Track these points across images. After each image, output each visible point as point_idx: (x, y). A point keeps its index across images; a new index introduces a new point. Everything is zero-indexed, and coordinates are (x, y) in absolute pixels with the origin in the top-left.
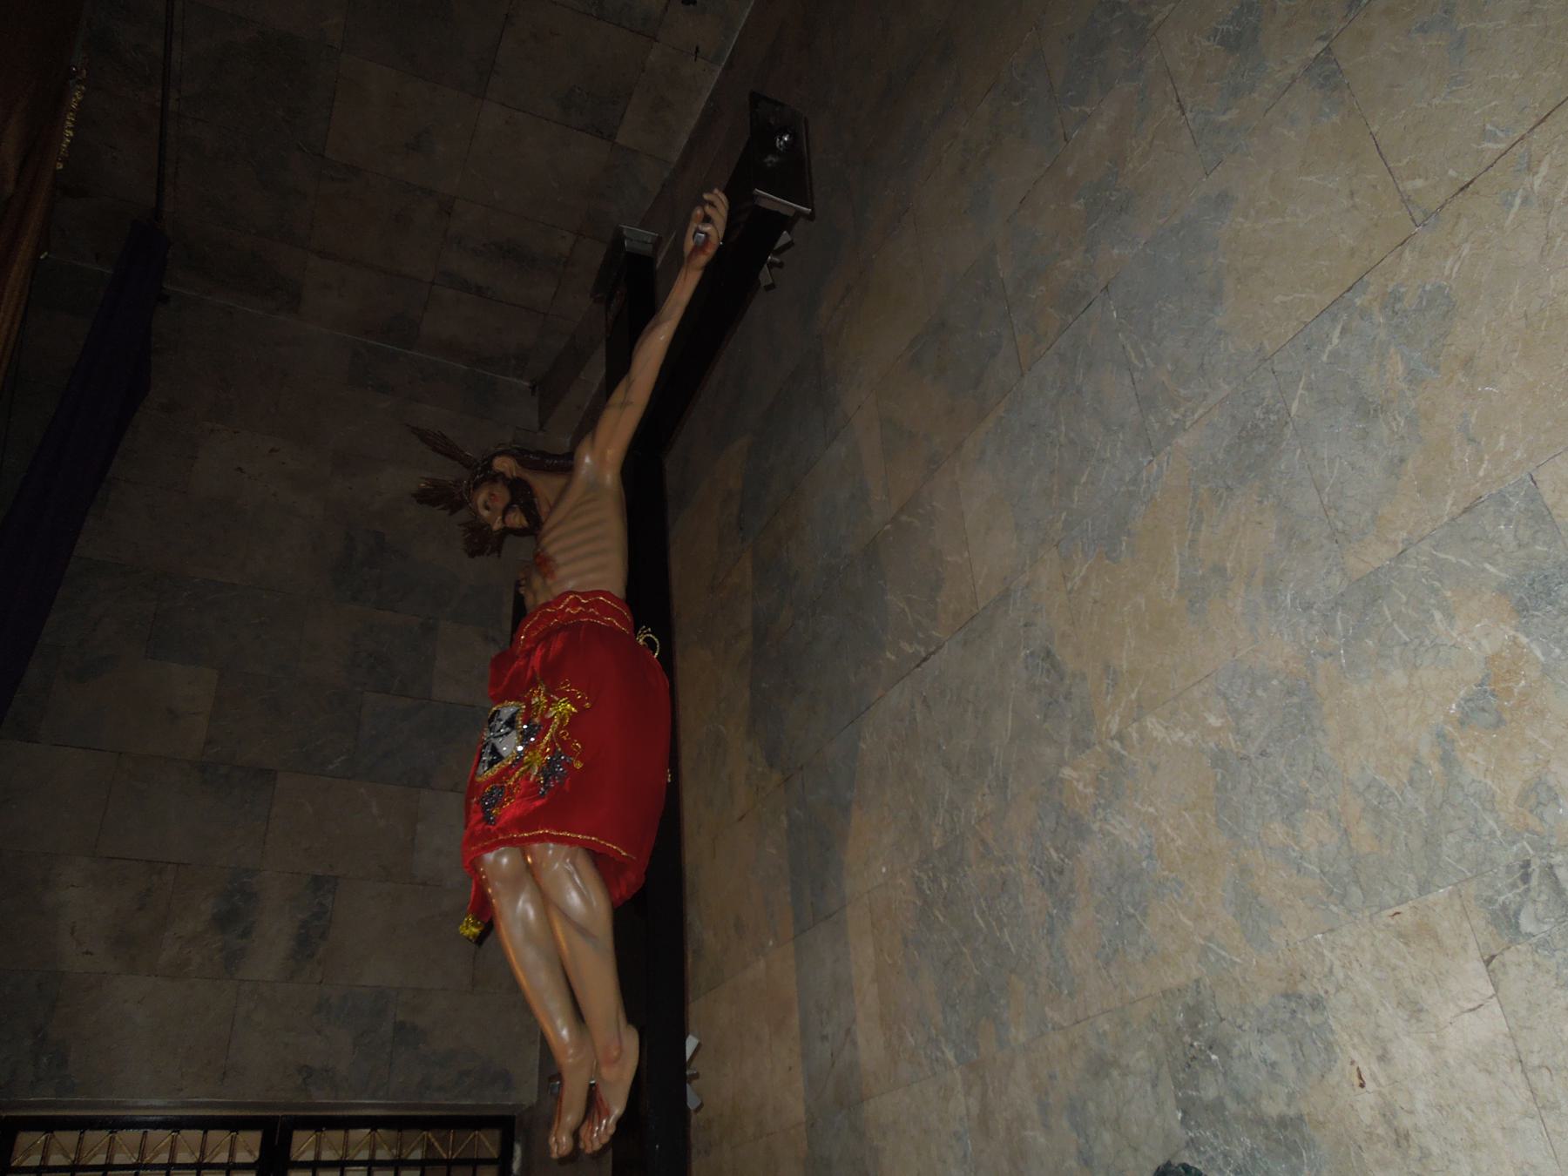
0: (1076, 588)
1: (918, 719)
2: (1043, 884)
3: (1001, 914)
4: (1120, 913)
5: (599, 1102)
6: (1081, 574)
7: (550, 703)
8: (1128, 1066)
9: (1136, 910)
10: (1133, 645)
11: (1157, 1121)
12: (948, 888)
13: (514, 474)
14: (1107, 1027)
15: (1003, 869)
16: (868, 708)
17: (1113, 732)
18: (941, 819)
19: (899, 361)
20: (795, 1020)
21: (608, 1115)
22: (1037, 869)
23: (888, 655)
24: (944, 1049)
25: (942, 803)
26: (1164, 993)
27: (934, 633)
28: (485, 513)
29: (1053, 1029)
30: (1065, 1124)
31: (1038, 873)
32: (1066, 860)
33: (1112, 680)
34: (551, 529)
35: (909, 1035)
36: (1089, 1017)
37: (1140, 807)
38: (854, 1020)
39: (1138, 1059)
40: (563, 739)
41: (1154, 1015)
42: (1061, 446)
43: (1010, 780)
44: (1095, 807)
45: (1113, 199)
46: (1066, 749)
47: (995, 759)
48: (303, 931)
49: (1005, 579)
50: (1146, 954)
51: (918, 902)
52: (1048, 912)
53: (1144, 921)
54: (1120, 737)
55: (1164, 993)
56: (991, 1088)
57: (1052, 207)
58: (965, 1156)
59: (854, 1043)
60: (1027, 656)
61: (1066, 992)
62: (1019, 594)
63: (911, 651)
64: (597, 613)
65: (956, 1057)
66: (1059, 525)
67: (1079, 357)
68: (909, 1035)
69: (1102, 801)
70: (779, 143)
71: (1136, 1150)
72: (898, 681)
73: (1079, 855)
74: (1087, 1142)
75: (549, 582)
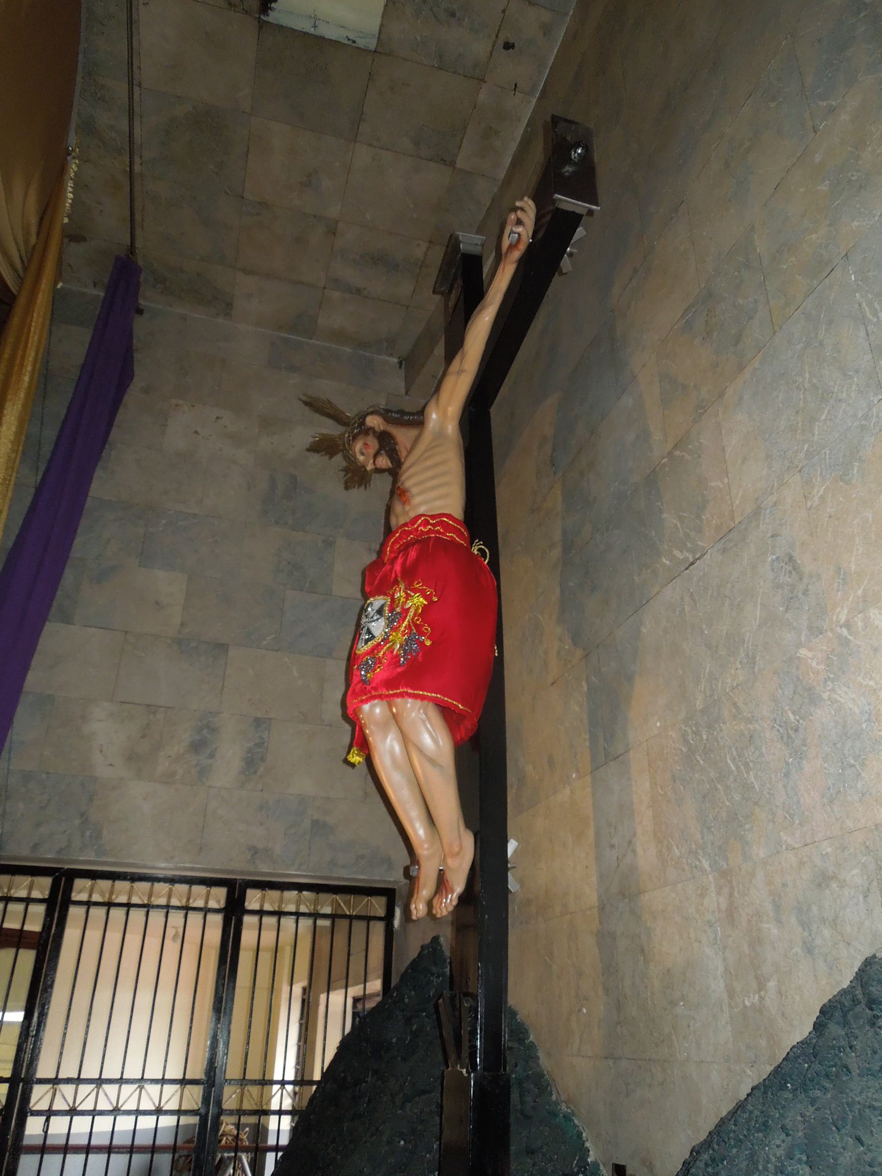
0: (814, 506)
1: (686, 610)
2: (782, 738)
3: (748, 760)
4: (843, 763)
5: (446, 883)
6: (820, 494)
7: (408, 597)
8: (844, 881)
9: (856, 761)
10: (860, 551)
11: (867, 923)
13: (382, 428)
14: (829, 850)
15: (751, 727)
16: (648, 602)
17: (842, 621)
18: (703, 688)
19: (675, 327)
20: (591, 832)
21: (452, 892)
22: (777, 727)
23: (664, 561)
25: (704, 675)
26: (876, 825)
27: (699, 543)
28: (361, 458)
29: (787, 849)
30: (793, 920)
31: (778, 730)
32: (801, 721)
33: (843, 579)
34: (410, 467)
35: (675, 848)
36: (815, 842)
37: (861, 681)
38: (635, 834)
39: (854, 875)
40: (417, 624)
41: (868, 844)
42: (805, 390)
43: (757, 659)
44: (825, 681)
45: (854, 178)
46: (804, 634)
47: (746, 641)
48: (250, 755)
49: (757, 499)
50: (863, 795)
51: (684, 750)
52: (785, 760)
53: (862, 770)
54: (848, 625)
55: (876, 825)
56: (736, 890)
57: (802, 190)
58: (715, 939)
59: (634, 851)
60: (773, 561)
61: (797, 822)
62: (768, 512)
63: (682, 558)
64: (441, 530)
65: (710, 866)
66: (802, 455)
67: (822, 316)
68: (675, 848)
69: (832, 676)
70: (574, 155)
71: (849, 944)
73: (811, 718)
74: (810, 935)
75: (407, 508)
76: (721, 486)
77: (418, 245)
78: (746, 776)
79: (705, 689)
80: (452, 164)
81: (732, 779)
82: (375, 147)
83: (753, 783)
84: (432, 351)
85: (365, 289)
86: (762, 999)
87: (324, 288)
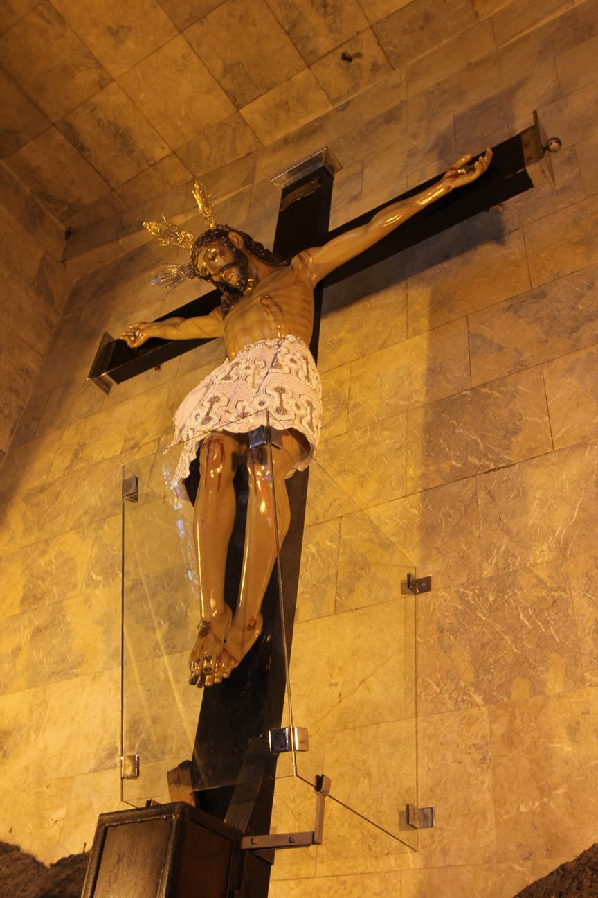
3: (548, 618)
12: (495, 601)
24: (471, 694)
51: (459, 607)
65: (484, 699)
72: (463, 479)
76: (540, 421)
77: (163, 148)
78: (544, 630)
79: (497, 562)
80: (239, 107)
81: (524, 631)
82: (193, 49)
83: (553, 635)
84: (117, 238)
85: (89, 150)
86: (543, 806)
87: (54, 125)
